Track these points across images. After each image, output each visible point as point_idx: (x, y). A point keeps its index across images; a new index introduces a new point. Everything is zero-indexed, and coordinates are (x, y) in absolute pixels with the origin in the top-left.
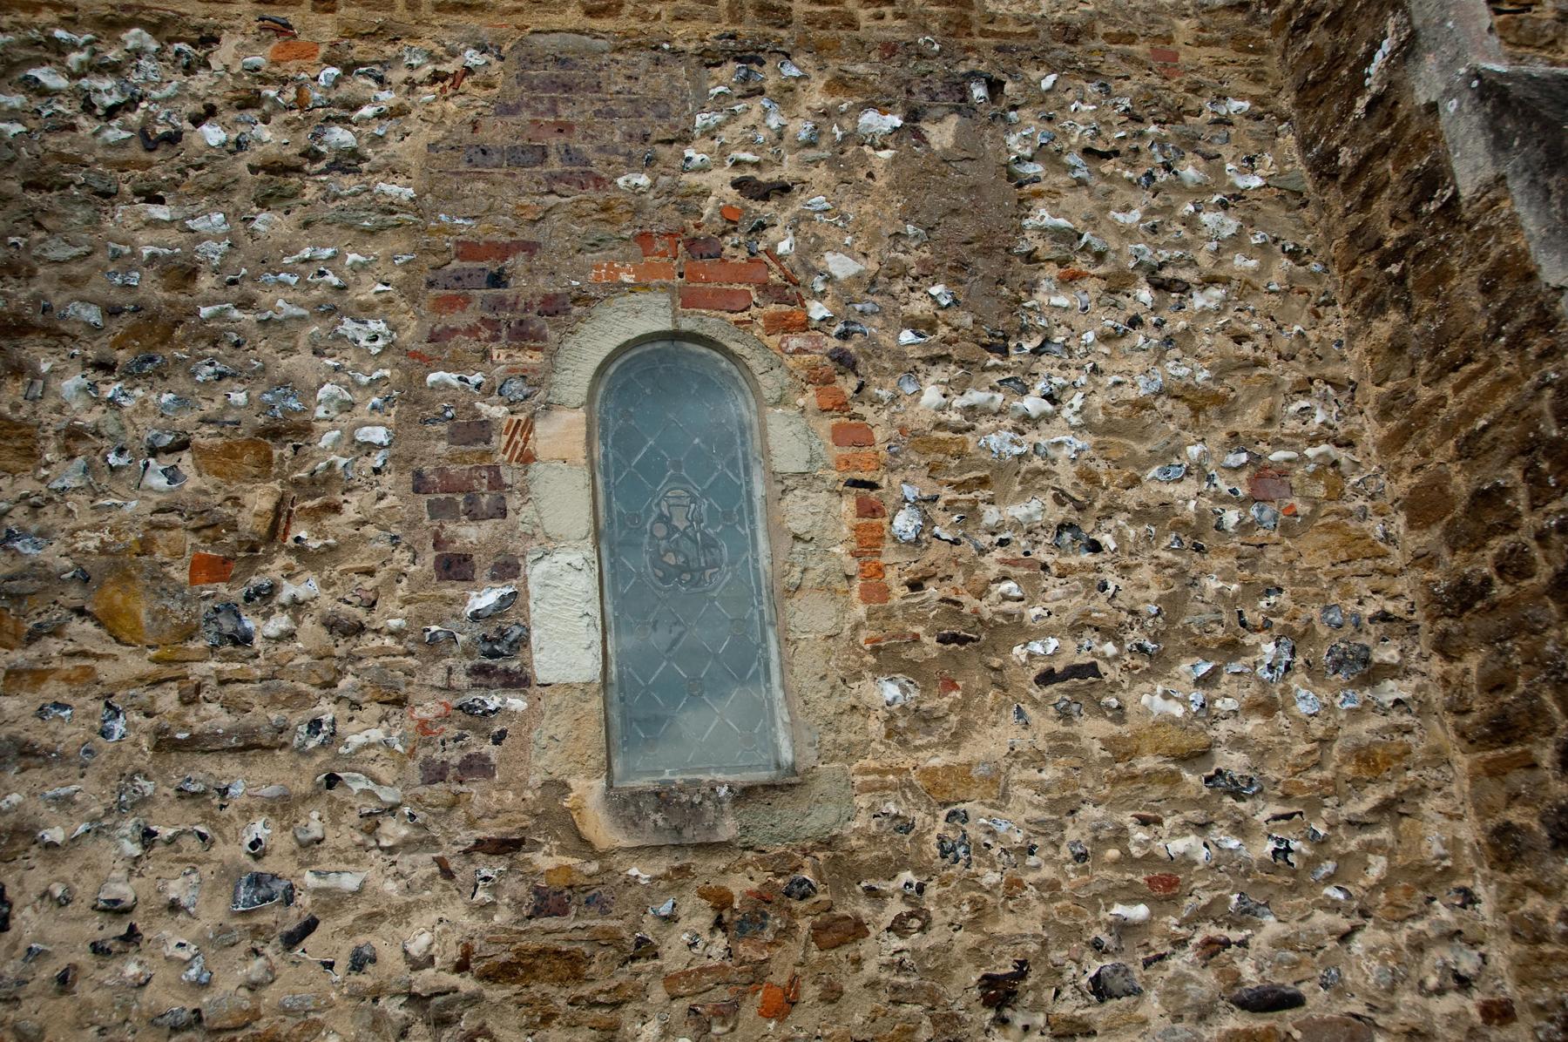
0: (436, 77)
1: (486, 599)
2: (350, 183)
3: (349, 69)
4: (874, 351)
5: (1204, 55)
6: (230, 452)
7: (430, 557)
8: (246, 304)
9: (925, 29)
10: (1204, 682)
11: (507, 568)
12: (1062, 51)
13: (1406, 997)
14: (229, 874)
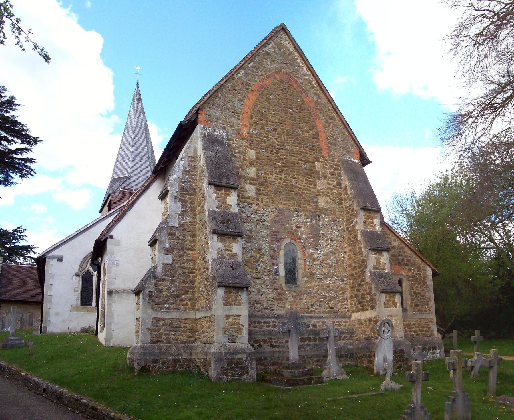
0: (272, 211)
1: (276, 268)
3: (264, 209)
4: (307, 246)
5: (338, 213)
6: (256, 251)
7: (271, 263)
8: (257, 236)
10: (330, 280)
11: (277, 265)
13: (342, 309)
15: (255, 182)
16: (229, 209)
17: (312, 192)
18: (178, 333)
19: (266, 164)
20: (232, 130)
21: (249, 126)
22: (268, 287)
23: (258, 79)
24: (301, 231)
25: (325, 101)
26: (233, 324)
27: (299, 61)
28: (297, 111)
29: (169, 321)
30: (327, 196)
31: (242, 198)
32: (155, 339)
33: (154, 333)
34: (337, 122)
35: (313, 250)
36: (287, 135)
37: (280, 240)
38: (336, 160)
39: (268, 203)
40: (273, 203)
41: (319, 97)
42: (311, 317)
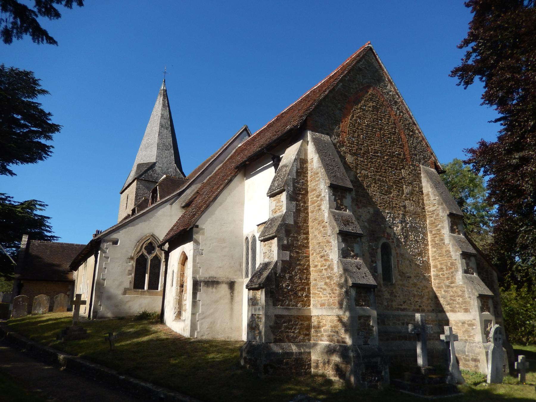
1: (374, 265)
11: (376, 262)
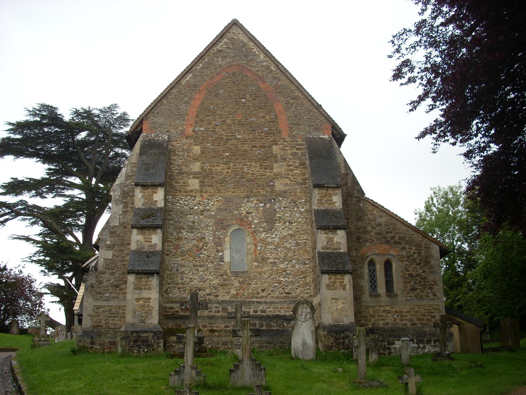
0: (217, 201)
1: (220, 254)
2: (209, 213)
3: (208, 200)
4: (258, 230)
5: (300, 194)
6: (199, 240)
8: (200, 226)
9: (268, 193)
11: (222, 251)
12: (283, 195)
13: (302, 294)
14: (199, 276)
15: (200, 175)
16: (155, 205)
17: (268, 176)
18: (117, 319)
19: (213, 157)
20: (177, 132)
21: (194, 124)
22: (212, 274)
23: (207, 78)
24: (252, 216)
25: (287, 82)
26: (143, 306)
27: (255, 50)
28: (251, 99)
29: (109, 308)
30: (287, 178)
31: (184, 192)
32: (95, 324)
33: (95, 319)
34: (301, 101)
35: (266, 234)
36: (238, 125)
37: (225, 228)
38: (300, 140)
39: (214, 194)
40: (219, 191)
41: (279, 80)
42: (259, 303)
